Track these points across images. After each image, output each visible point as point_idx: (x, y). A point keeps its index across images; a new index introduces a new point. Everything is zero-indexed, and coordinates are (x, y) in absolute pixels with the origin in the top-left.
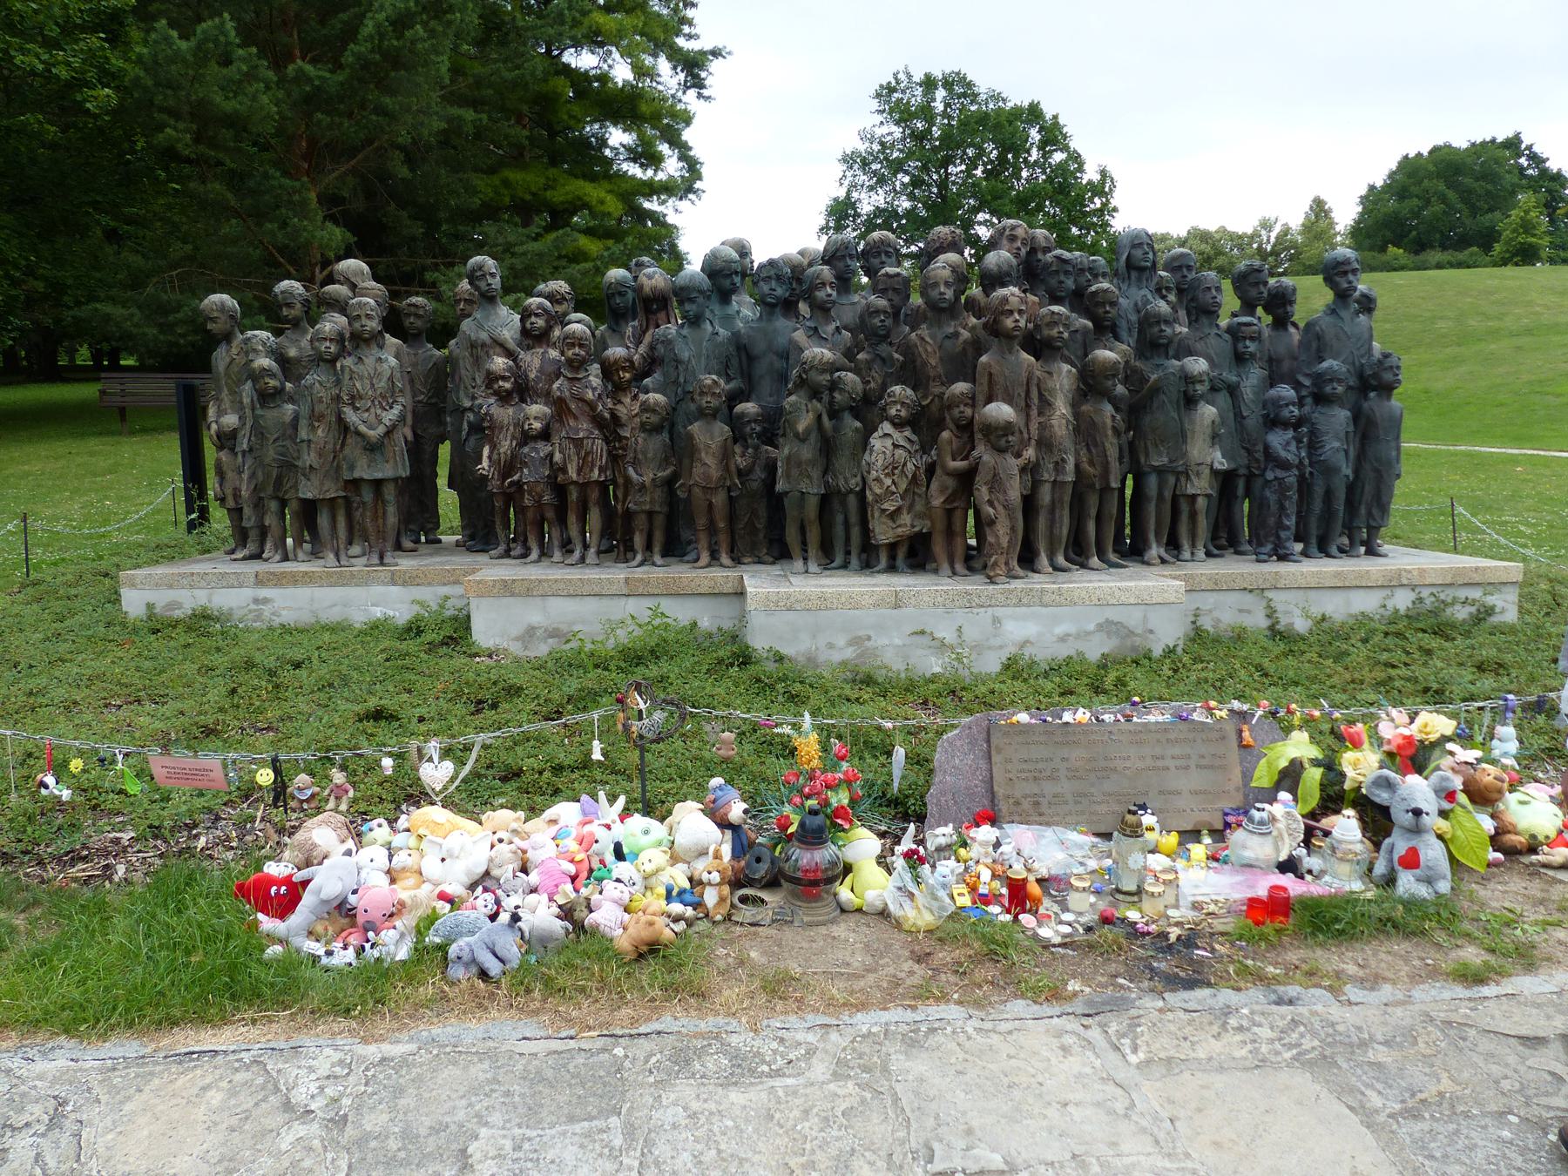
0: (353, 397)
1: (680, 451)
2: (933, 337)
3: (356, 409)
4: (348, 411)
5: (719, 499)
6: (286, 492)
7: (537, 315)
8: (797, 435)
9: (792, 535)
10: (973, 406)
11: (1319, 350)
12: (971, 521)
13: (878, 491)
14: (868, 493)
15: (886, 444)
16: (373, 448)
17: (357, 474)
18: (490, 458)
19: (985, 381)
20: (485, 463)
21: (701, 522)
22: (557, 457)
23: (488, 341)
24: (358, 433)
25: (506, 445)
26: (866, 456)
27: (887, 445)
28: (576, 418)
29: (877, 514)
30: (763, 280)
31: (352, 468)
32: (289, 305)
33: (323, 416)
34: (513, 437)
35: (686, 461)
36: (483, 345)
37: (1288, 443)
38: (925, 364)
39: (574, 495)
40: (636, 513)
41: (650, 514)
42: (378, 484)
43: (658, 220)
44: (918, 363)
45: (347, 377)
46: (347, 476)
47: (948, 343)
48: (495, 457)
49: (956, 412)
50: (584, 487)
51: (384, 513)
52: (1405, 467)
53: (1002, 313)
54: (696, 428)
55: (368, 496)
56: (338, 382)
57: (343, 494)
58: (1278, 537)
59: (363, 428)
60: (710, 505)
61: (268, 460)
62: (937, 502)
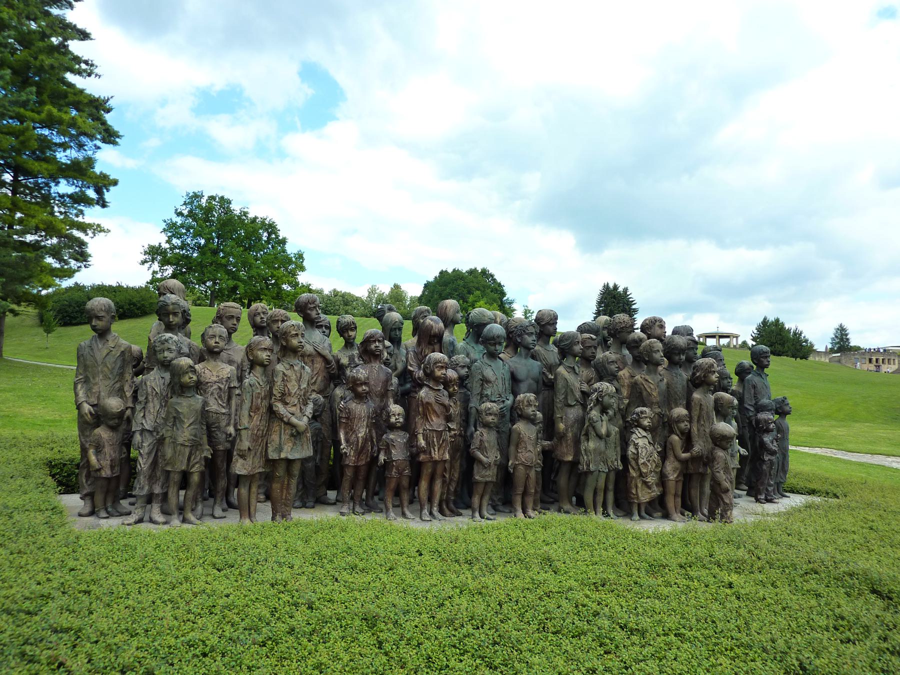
0: (283, 394)
1: (508, 442)
2: (654, 380)
3: (286, 404)
4: (280, 407)
5: (532, 474)
6: (193, 466)
7: (379, 341)
8: (599, 437)
9: (588, 497)
10: (690, 422)
11: (755, 393)
12: (707, 490)
13: (645, 471)
14: (631, 471)
15: (641, 440)
16: (297, 435)
17: (283, 456)
18: (347, 441)
19: (698, 408)
20: (344, 445)
21: (520, 490)
22: (422, 442)
23: (314, 353)
24: (289, 424)
25: (362, 433)
26: (632, 449)
27: (641, 440)
28: (438, 416)
29: (639, 485)
30: (527, 334)
31: (280, 449)
32: (175, 314)
33: (258, 409)
34: (367, 426)
35: (512, 448)
36: (309, 356)
37: (772, 443)
38: (650, 395)
39: (427, 471)
40: (478, 482)
41: (486, 483)
42: (289, 462)
43: (82, 244)
44: (645, 393)
45: (278, 380)
46: (273, 455)
47: (660, 384)
48: (353, 438)
49: (682, 425)
50: (436, 463)
51: (288, 484)
52: (790, 454)
53: (710, 372)
54: (521, 426)
55: (280, 472)
56: (271, 383)
57: (261, 470)
58: (767, 490)
59: (294, 420)
60: (528, 478)
61: (180, 440)
62: (672, 477)
